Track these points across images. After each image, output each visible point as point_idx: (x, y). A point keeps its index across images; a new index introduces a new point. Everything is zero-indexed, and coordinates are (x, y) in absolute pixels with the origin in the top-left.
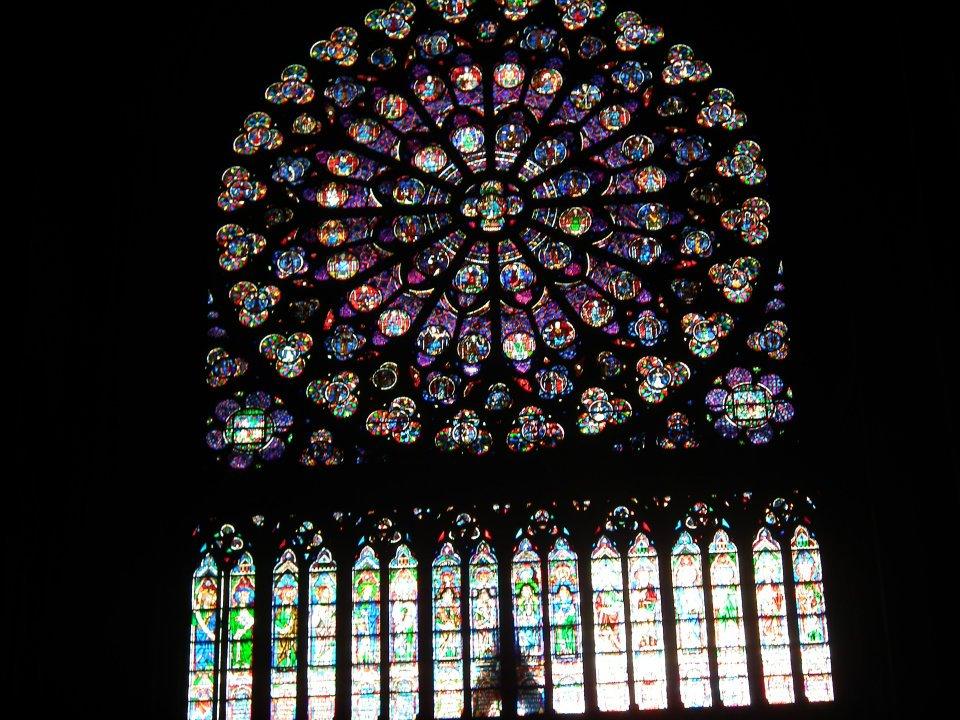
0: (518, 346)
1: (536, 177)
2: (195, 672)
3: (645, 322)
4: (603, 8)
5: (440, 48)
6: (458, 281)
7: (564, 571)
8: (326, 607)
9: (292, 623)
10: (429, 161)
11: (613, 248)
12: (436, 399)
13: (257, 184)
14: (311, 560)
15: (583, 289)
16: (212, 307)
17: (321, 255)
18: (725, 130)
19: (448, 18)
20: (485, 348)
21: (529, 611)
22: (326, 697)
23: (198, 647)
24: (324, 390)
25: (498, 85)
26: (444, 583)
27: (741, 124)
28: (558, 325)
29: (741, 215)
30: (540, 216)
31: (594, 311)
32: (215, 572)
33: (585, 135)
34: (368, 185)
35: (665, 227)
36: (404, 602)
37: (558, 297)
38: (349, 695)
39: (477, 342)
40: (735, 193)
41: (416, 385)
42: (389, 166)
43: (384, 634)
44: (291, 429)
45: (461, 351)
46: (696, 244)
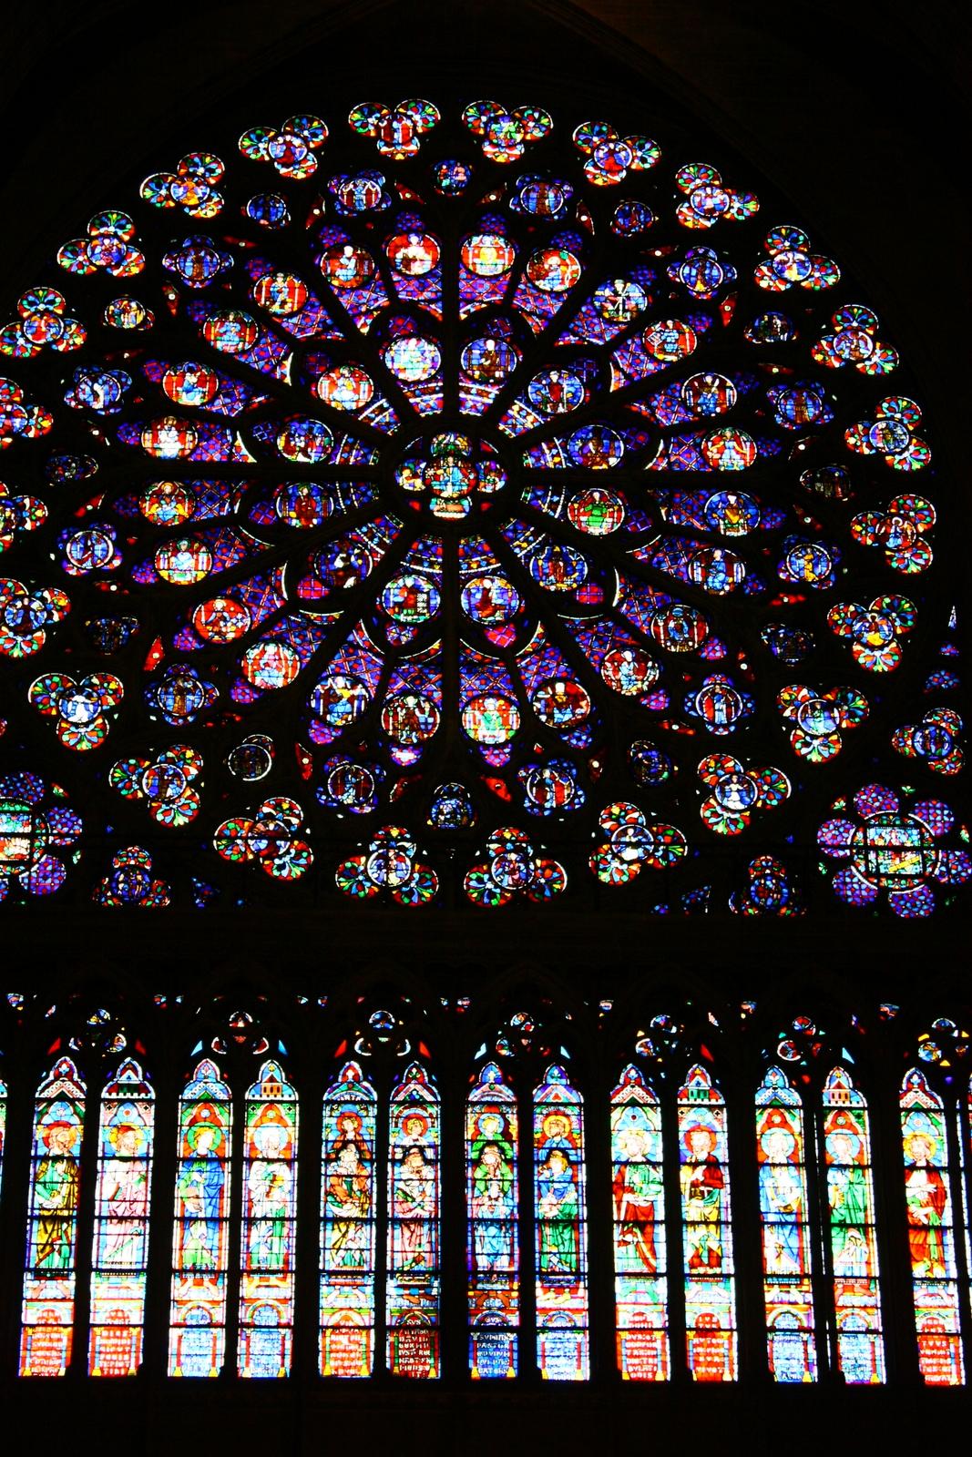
1: (529, 431)
4: (655, 154)
6: (387, 599)
7: (559, 1126)
8: (128, 1165)
9: (65, 1189)
11: (659, 563)
12: (340, 803)
13: (36, 410)
15: (607, 629)
17: (147, 541)
19: (384, 149)
20: (431, 720)
21: (494, 1191)
25: (468, 271)
26: (344, 1132)
27: (888, 367)
28: (560, 688)
29: (885, 521)
31: (626, 669)
35: (752, 533)
36: (269, 1161)
37: (561, 642)
39: (416, 710)
40: (879, 486)
41: (306, 776)
43: (237, 1220)
45: (387, 722)
46: (805, 567)
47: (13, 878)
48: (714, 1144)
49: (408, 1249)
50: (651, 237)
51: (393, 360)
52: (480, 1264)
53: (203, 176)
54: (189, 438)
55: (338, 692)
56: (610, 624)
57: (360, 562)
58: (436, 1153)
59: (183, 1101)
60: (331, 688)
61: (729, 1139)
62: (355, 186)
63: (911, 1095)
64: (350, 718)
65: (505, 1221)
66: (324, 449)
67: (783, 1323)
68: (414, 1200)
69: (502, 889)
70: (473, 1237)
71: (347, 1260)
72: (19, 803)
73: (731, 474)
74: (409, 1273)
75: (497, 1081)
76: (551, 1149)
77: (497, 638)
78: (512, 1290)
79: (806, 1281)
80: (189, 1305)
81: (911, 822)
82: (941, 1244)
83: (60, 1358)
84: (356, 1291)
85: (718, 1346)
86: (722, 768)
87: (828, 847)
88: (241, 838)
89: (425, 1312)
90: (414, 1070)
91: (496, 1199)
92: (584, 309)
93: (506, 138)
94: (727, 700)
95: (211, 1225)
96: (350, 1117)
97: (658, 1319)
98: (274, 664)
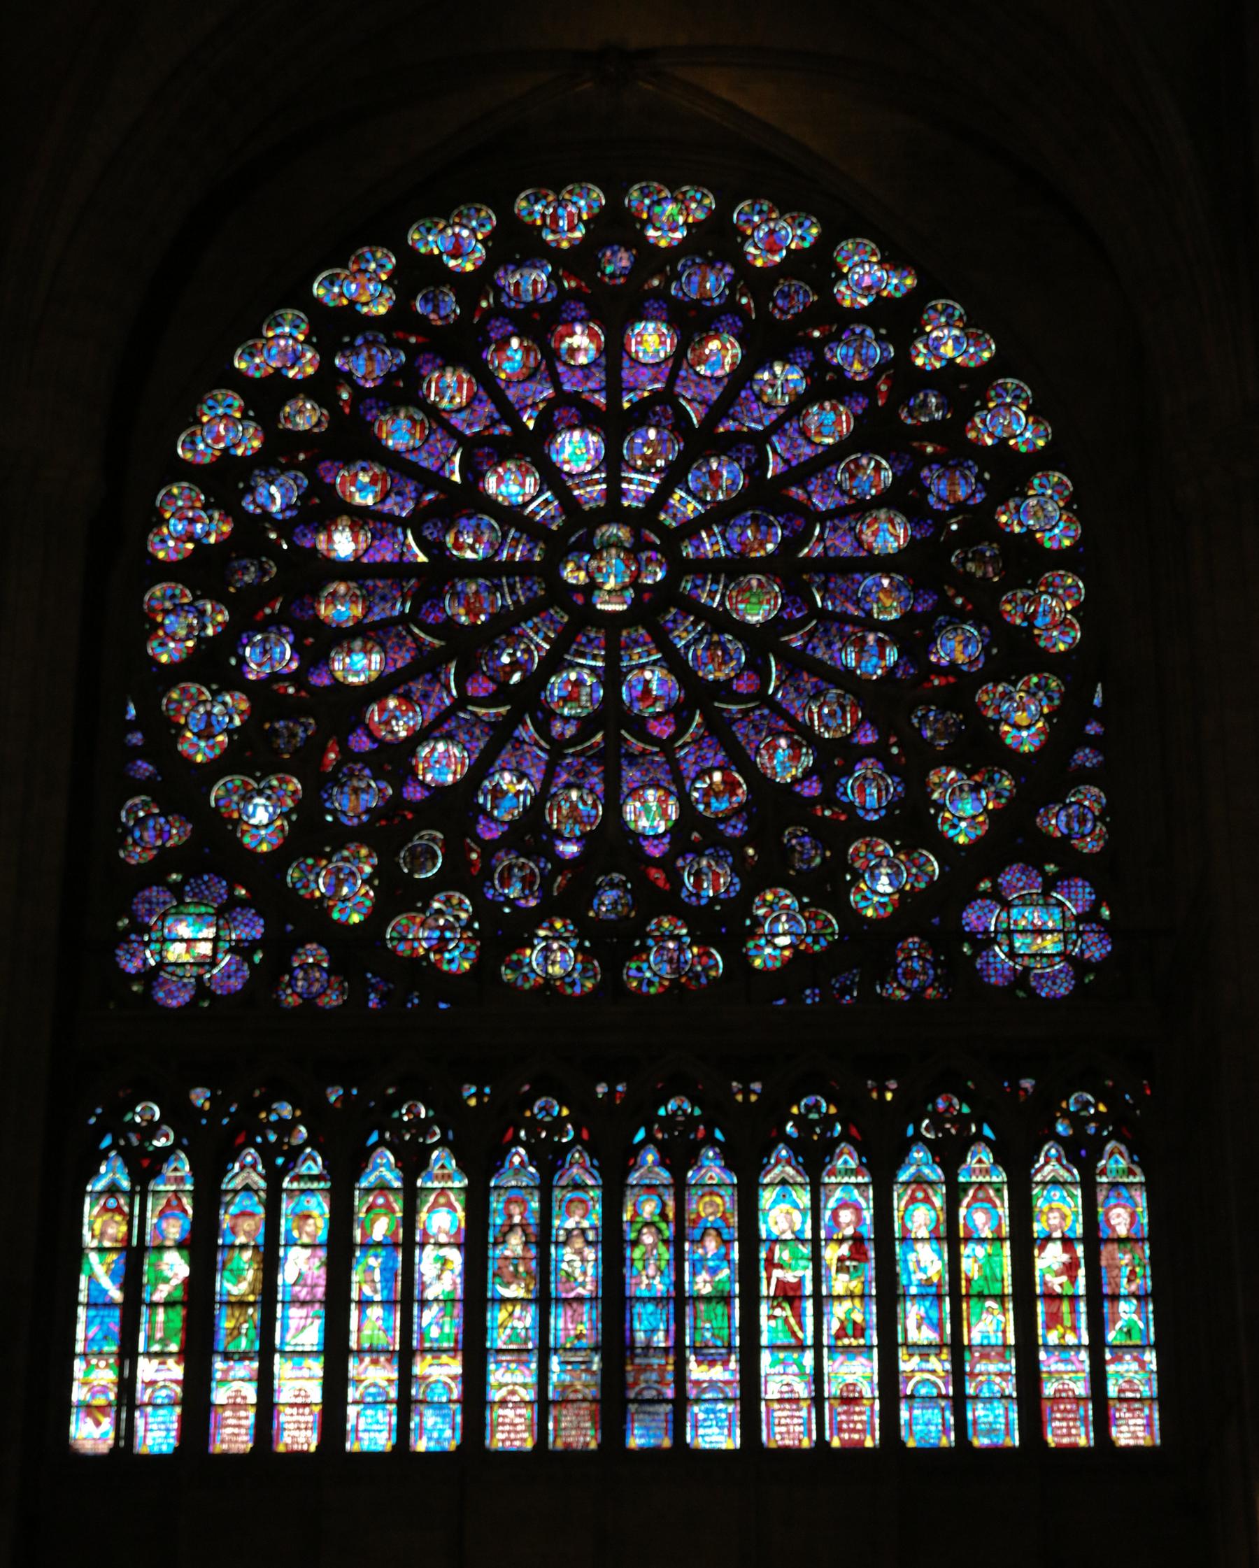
0: (647, 810)
3: (865, 778)
4: (814, 231)
5: (535, 291)
7: (713, 1205)
8: (308, 1252)
9: (250, 1275)
10: (509, 485)
11: (814, 649)
12: (506, 897)
13: (216, 515)
14: (285, 1170)
15: (762, 716)
16: (133, 726)
17: (320, 642)
18: (1014, 450)
19: (550, 237)
20: (593, 812)
21: (651, 1271)
23: (92, 1313)
24: (318, 875)
25: (631, 359)
26: (510, 1216)
27: (1041, 443)
28: (717, 776)
29: (1035, 600)
30: (695, 587)
34: (404, 523)
35: (905, 617)
36: (441, 1245)
37: (718, 729)
38: (344, 1403)
39: (578, 802)
40: (1027, 561)
42: (442, 491)
44: (254, 945)
46: (956, 648)
47: (199, 978)
48: (859, 1220)
50: (810, 316)
54: (361, 537)
56: (766, 711)
63: (1048, 1168)
65: (661, 1298)
66: (491, 544)
67: (923, 1391)
69: (661, 978)
75: (654, 1163)
76: (706, 1229)
79: (945, 1351)
80: (366, 1383)
82: (1074, 1311)
85: (860, 1413)
89: (586, 1386)
92: (743, 394)
93: (670, 220)
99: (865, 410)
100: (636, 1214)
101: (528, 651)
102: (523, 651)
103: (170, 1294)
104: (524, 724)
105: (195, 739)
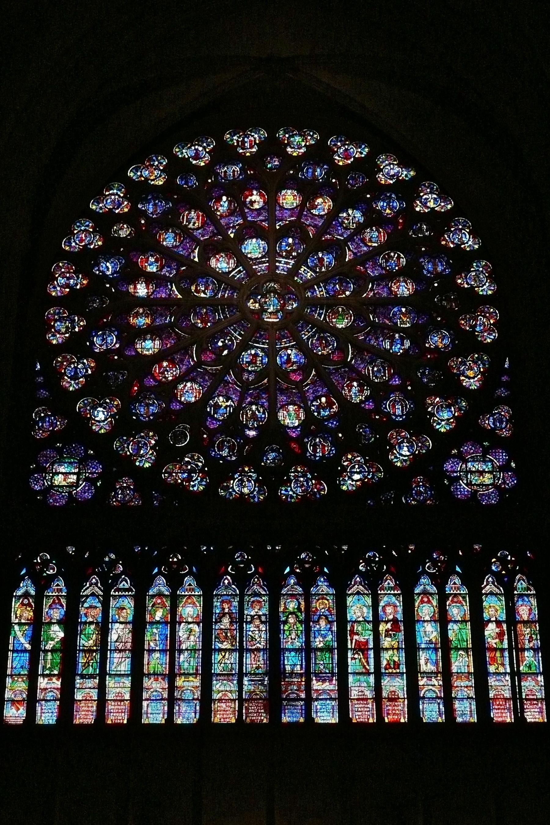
0: (290, 415)
2: (11, 675)
3: (395, 401)
4: (367, 150)
5: (234, 175)
6: (243, 360)
10: (221, 264)
11: (370, 340)
12: (221, 455)
13: (80, 276)
16: (39, 373)
18: (464, 250)
19: (241, 151)
20: (263, 416)
22: (121, 701)
23: (15, 655)
24: (129, 445)
26: (223, 609)
27: (476, 247)
28: (323, 400)
29: (476, 319)
31: (354, 390)
32: (33, 593)
33: (349, 250)
35: (413, 325)
40: (472, 301)
43: (173, 649)
46: (437, 341)
47: (70, 493)
48: (396, 612)
49: (253, 663)
50: (366, 188)
51: (245, 249)
52: (287, 669)
53: (157, 165)
54: (150, 287)
55: (220, 404)
56: (347, 369)
57: (230, 343)
58: (266, 618)
59: (148, 595)
60: (217, 402)
61: (404, 610)
62: (228, 168)
63: (488, 587)
64: (225, 416)
65: (299, 648)
66: (213, 291)
67: (429, 695)
68: (256, 640)
69: (297, 494)
70: (284, 657)
71: (225, 668)
72: (72, 458)
73: (403, 298)
74: (254, 674)
75: (295, 584)
76: (320, 615)
77: (293, 377)
78: (302, 681)
79: (439, 675)
80: (152, 690)
81: (487, 459)
83: (93, 715)
84: (229, 683)
86: (399, 436)
87: (448, 472)
88: (175, 473)
89: (262, 692)
90: (256, 580)
91: (294, 639)
92: (334, 223)
93: (298, 145)
94: (402, 403)
95: (162, 653)
96: (226, 602)
97: (369, 694)
98: (190, 392)
99: (392, 231)
100: (286, 608)
101: (231, 340)
102: (229, 340)
103: (54, 646)
104: (230, 374)
105: (69, 380)
